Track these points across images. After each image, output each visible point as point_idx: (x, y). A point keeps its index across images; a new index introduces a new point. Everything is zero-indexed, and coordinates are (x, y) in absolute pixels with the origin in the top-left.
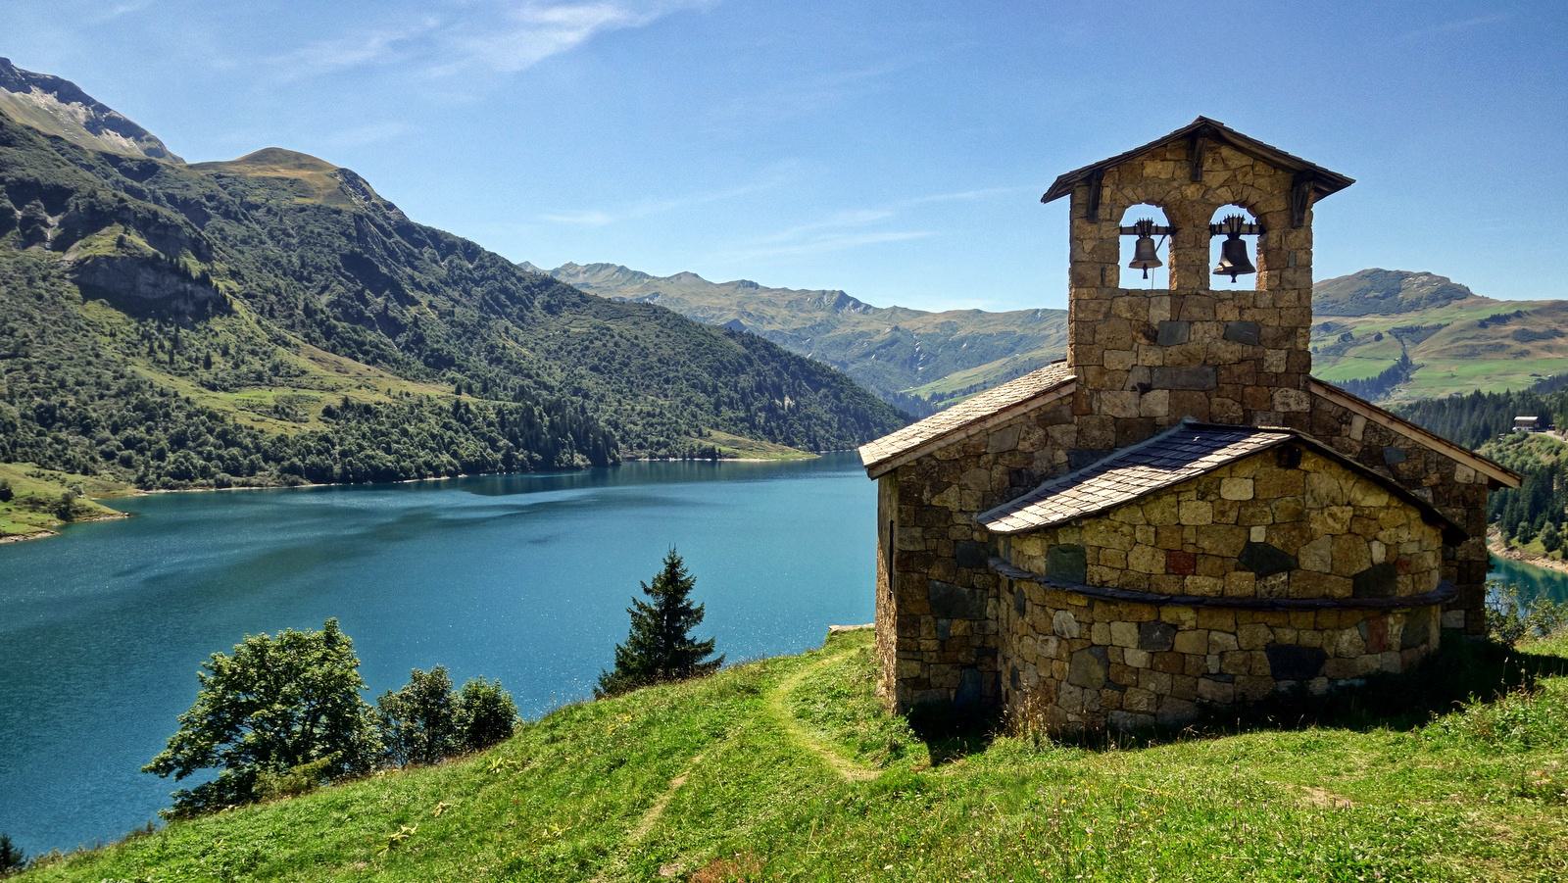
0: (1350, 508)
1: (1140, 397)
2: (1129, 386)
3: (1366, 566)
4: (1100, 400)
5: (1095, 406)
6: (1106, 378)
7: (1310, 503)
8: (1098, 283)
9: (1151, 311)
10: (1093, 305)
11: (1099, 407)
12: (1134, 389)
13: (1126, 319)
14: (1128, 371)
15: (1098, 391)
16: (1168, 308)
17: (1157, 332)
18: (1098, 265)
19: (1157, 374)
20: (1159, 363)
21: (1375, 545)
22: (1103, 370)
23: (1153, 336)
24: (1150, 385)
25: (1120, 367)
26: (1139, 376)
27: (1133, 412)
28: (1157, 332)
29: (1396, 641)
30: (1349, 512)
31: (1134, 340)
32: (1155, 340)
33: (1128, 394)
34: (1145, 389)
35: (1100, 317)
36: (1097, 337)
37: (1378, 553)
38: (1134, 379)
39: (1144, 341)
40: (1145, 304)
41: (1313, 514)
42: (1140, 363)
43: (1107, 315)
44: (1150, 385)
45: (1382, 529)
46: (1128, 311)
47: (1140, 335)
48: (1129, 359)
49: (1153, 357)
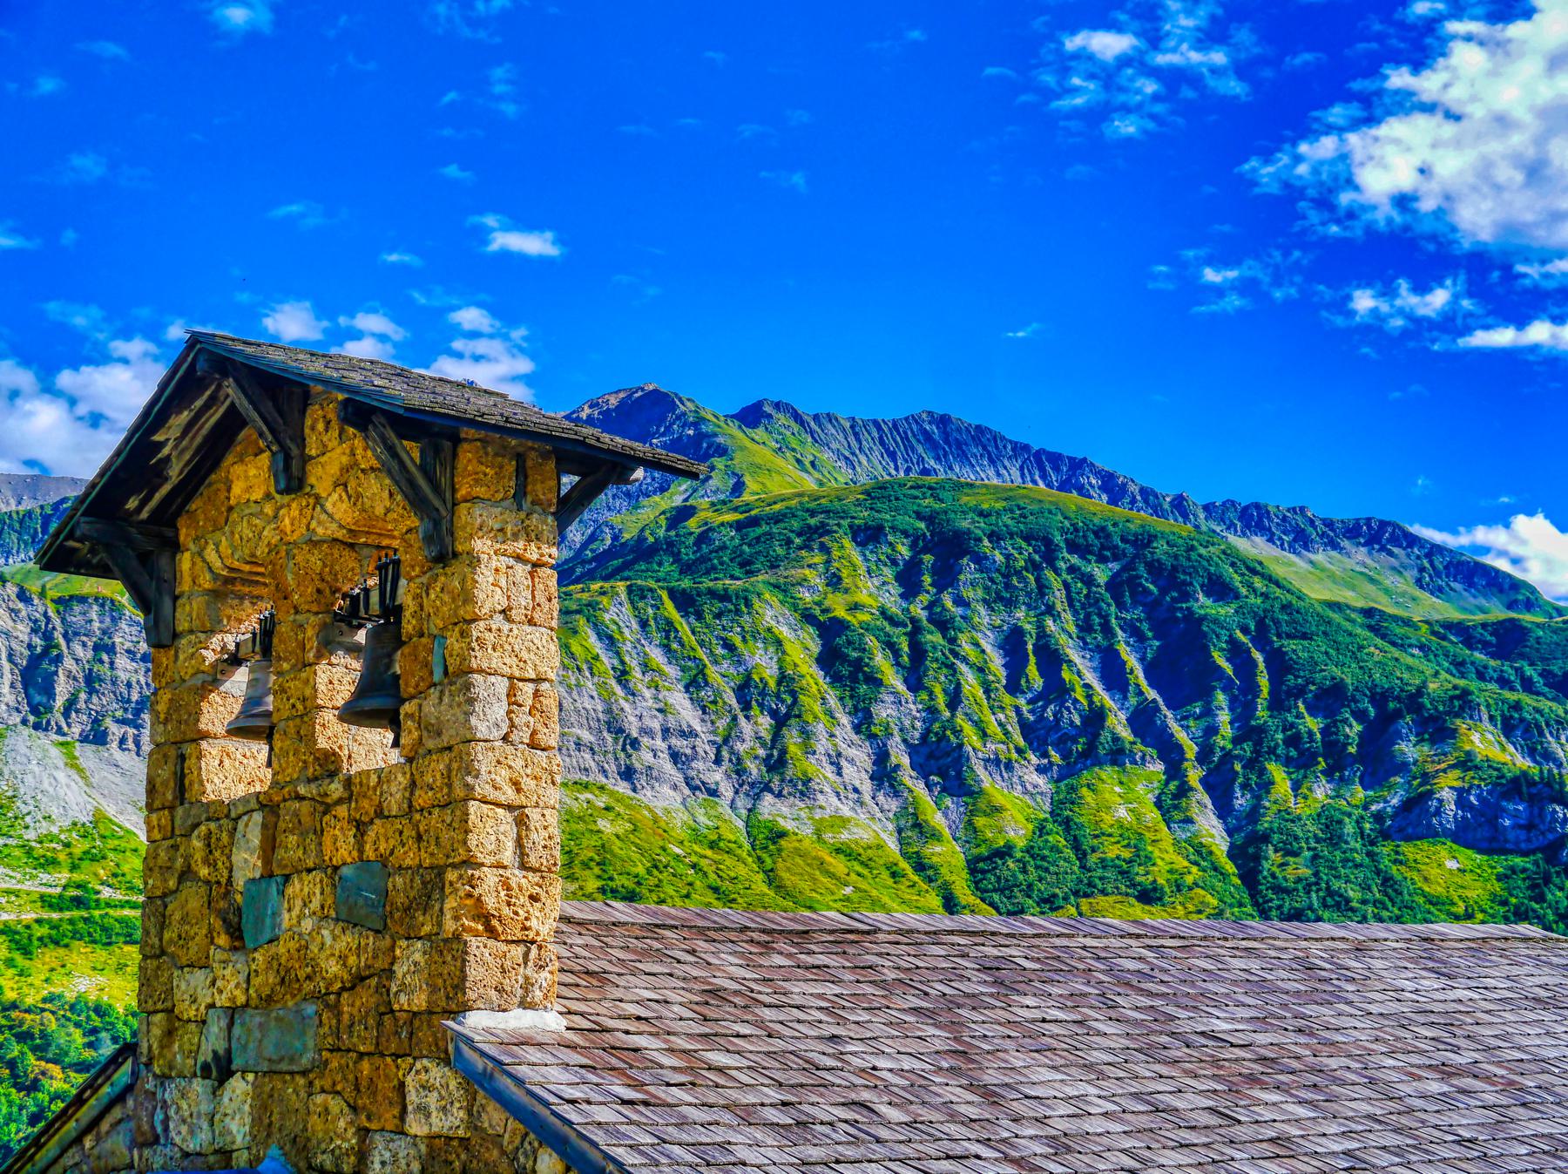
8: (169, 796)
12: (206, 1071)
13: (208, 882)
15: (163, 1078)
34: (220, 1070)
35: (172, 884)
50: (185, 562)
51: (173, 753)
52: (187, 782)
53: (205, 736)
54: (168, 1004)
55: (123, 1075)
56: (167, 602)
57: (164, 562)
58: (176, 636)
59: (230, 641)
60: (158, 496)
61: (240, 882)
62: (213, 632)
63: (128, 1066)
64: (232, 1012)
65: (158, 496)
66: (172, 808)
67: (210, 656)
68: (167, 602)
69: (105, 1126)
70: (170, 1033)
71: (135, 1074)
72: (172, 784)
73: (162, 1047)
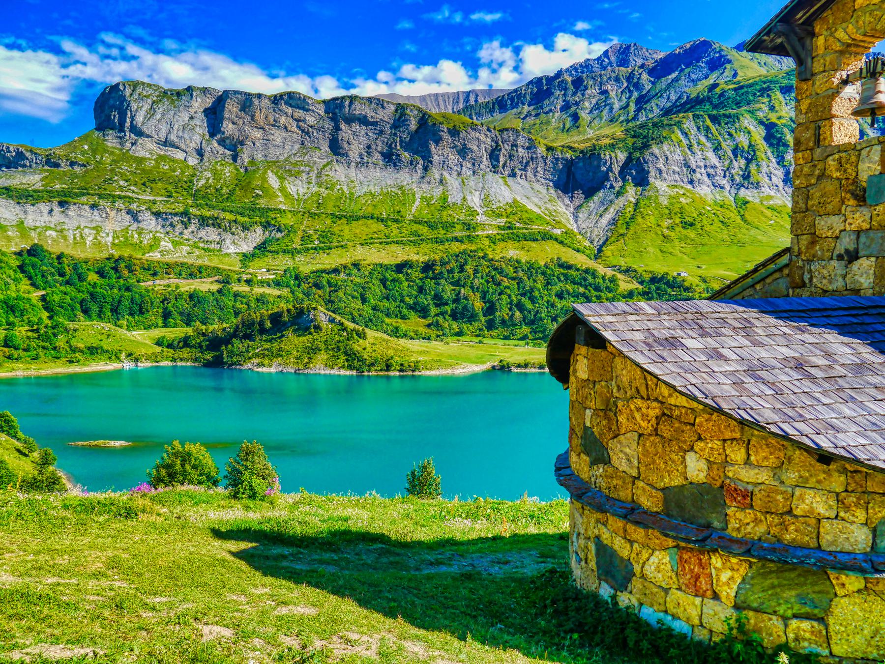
0: (655, 404)
1: (846, 267)
2: (835, 257)
3: (677, 481)
4: (810, 271)
5: (806, 277)
6: (817, 248)
7: (615, 393)
8: (811, 144)
9: (861, 166)
10: (806, 170)
11: (811, 280)
12: (840, 257)
13: (838, 179)
14: (837, 238)
15: (809, 261)
16: (877, 158)
17: (865, 190)
18: (812, 126)
19: (863, 239)
20: (866, 226)
21: (691, 458)
22: (815, 238)
23: (861, 198)
24: (857, 251)
25: (829, 234)
26: (847, 243)
27: (839, 284)
28: (865, 190)
29: (728, 592)
30: (654, 411)
31: (843, 202)
32: (864, 201)
33: (835, 263)
34: (852, 256)
35: (813, 181)
36: (810, 203)
37: (696, 468)
38: (840, 249)
39: (852, 202)
40: (853, 158)
41: (620, 404)
42: (848, 228)
43: (822, 176)
44: (857, 251)
45: (700, 438)
46: (837, 170)
47: (848, 196)
48: (836, 222)
49: (859, 219)
50: (820, 41)
51: (812, 126)
52: (821, 138)
53: (834, 116)
54: (813, 231)
55: (784, 260)
56: (809, 60)
57: (808, 42)
58: (813, 75)
59: (844, 74)
60: (815, 8)
61: (864, 176)
62: (836, 70)
63: (787, 256)
64: (858, 233)
65: (815, 8)
66: (811, 150)
67: (836, 81)
68: (809, 60)
69: (768, 281)
70: (813, 243)
71: (790, 260)
72: (813, 139)
73: (807, 248)
